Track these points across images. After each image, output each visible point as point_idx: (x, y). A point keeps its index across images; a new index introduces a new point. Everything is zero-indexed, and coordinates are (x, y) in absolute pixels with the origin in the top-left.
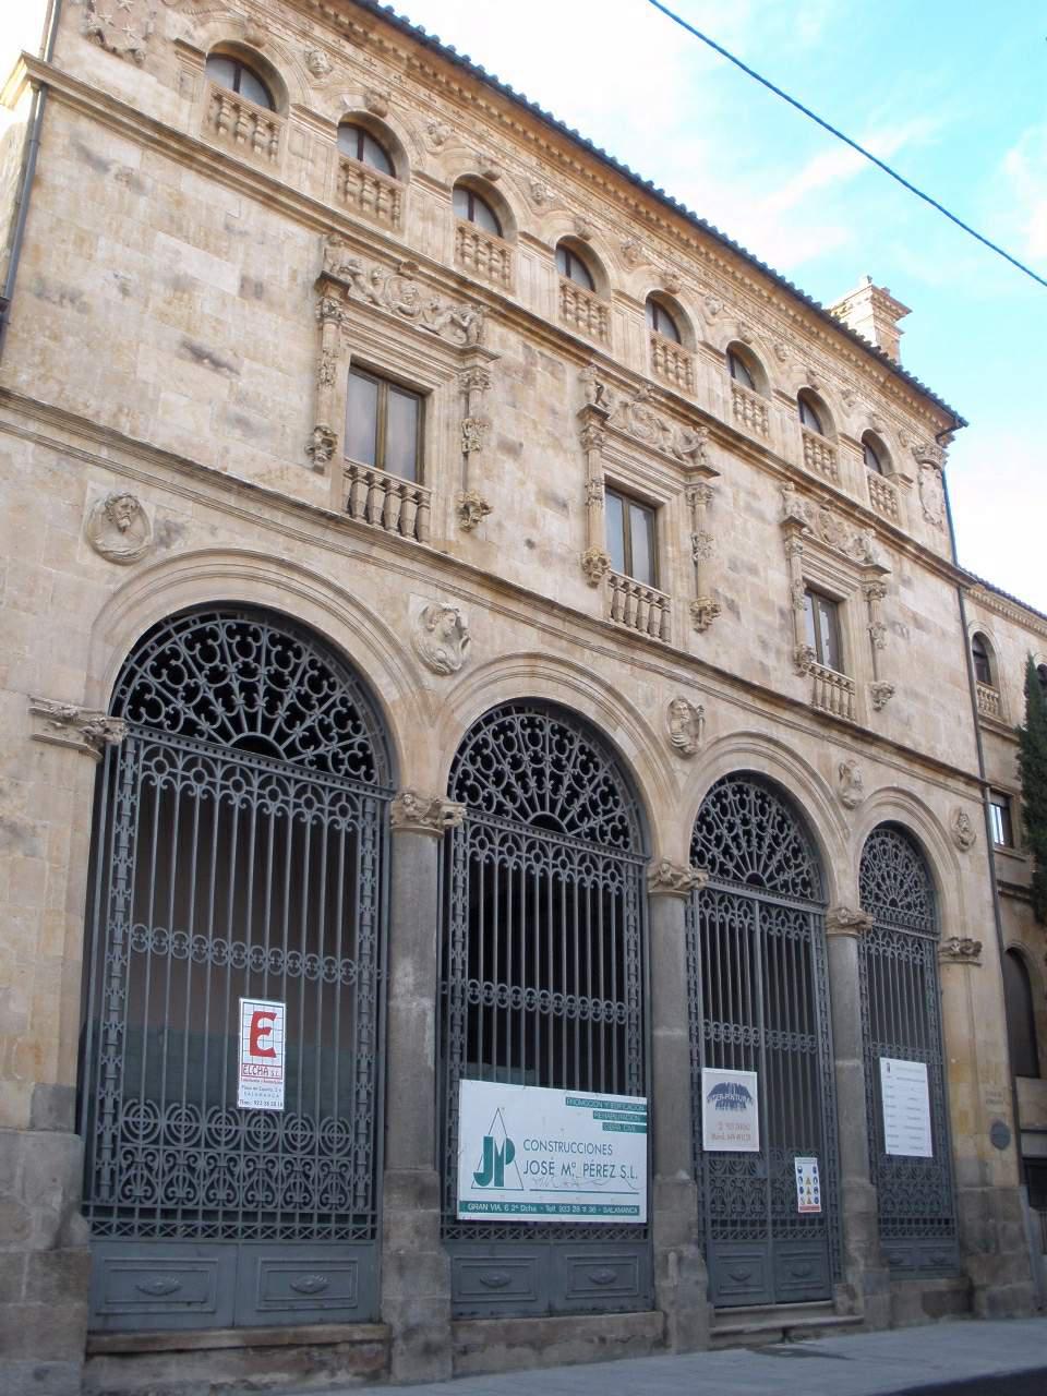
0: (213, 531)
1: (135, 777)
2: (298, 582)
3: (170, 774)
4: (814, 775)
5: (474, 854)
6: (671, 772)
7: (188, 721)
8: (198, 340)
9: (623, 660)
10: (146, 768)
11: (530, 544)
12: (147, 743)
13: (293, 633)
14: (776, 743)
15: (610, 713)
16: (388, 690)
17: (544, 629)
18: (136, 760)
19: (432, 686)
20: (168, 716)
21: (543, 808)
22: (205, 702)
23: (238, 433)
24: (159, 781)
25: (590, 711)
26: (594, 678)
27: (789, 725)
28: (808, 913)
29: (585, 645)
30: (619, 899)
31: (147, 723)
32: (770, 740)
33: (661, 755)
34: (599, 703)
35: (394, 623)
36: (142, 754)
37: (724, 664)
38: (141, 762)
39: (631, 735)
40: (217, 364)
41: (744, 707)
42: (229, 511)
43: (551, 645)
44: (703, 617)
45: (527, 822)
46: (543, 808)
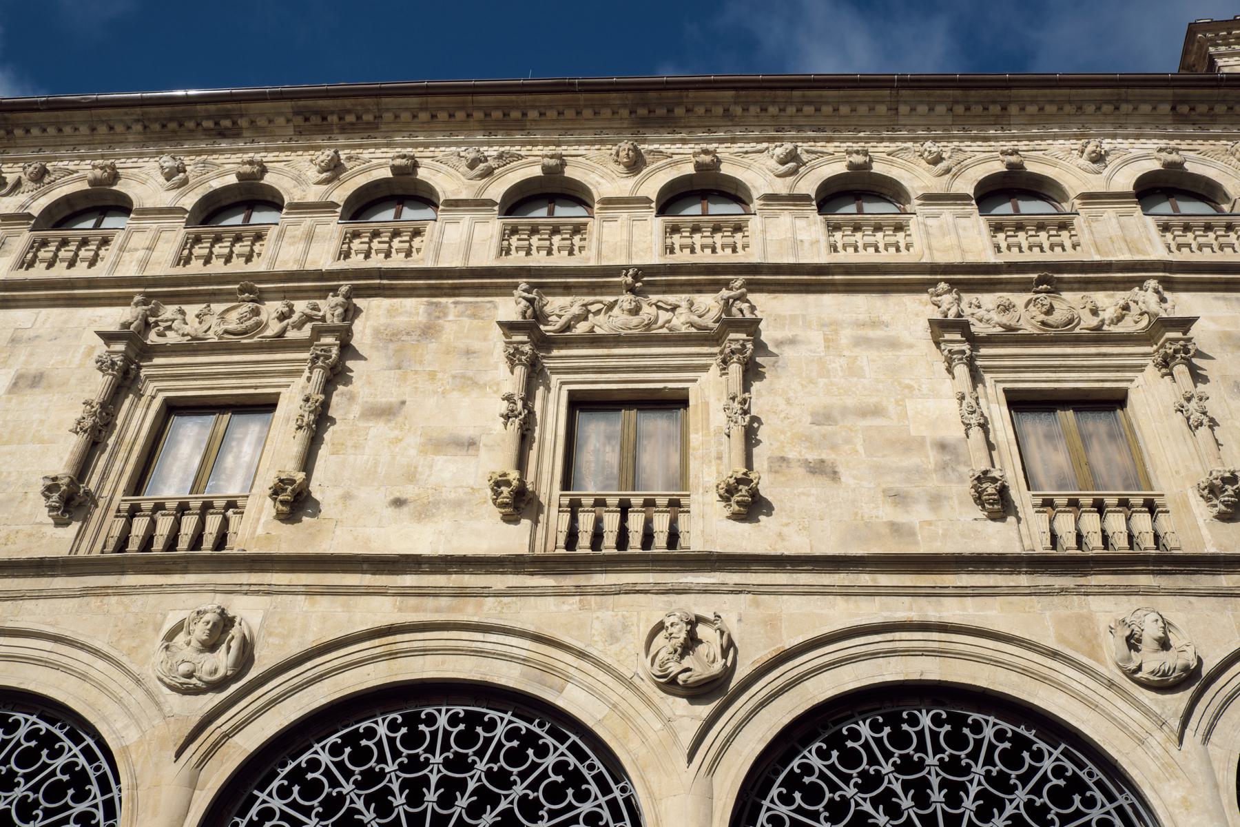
4: (1054, 655)
9: (560, 593)
11: (398, 503)
15: (547, 669)
16: (116, 729)
17: (403, 593)
19: (176, 710)
27: (961, 593)
33: (649, 702)
35: (131, 651)
39: (591, 690)
41: (824, 592)
43: (416, 609)
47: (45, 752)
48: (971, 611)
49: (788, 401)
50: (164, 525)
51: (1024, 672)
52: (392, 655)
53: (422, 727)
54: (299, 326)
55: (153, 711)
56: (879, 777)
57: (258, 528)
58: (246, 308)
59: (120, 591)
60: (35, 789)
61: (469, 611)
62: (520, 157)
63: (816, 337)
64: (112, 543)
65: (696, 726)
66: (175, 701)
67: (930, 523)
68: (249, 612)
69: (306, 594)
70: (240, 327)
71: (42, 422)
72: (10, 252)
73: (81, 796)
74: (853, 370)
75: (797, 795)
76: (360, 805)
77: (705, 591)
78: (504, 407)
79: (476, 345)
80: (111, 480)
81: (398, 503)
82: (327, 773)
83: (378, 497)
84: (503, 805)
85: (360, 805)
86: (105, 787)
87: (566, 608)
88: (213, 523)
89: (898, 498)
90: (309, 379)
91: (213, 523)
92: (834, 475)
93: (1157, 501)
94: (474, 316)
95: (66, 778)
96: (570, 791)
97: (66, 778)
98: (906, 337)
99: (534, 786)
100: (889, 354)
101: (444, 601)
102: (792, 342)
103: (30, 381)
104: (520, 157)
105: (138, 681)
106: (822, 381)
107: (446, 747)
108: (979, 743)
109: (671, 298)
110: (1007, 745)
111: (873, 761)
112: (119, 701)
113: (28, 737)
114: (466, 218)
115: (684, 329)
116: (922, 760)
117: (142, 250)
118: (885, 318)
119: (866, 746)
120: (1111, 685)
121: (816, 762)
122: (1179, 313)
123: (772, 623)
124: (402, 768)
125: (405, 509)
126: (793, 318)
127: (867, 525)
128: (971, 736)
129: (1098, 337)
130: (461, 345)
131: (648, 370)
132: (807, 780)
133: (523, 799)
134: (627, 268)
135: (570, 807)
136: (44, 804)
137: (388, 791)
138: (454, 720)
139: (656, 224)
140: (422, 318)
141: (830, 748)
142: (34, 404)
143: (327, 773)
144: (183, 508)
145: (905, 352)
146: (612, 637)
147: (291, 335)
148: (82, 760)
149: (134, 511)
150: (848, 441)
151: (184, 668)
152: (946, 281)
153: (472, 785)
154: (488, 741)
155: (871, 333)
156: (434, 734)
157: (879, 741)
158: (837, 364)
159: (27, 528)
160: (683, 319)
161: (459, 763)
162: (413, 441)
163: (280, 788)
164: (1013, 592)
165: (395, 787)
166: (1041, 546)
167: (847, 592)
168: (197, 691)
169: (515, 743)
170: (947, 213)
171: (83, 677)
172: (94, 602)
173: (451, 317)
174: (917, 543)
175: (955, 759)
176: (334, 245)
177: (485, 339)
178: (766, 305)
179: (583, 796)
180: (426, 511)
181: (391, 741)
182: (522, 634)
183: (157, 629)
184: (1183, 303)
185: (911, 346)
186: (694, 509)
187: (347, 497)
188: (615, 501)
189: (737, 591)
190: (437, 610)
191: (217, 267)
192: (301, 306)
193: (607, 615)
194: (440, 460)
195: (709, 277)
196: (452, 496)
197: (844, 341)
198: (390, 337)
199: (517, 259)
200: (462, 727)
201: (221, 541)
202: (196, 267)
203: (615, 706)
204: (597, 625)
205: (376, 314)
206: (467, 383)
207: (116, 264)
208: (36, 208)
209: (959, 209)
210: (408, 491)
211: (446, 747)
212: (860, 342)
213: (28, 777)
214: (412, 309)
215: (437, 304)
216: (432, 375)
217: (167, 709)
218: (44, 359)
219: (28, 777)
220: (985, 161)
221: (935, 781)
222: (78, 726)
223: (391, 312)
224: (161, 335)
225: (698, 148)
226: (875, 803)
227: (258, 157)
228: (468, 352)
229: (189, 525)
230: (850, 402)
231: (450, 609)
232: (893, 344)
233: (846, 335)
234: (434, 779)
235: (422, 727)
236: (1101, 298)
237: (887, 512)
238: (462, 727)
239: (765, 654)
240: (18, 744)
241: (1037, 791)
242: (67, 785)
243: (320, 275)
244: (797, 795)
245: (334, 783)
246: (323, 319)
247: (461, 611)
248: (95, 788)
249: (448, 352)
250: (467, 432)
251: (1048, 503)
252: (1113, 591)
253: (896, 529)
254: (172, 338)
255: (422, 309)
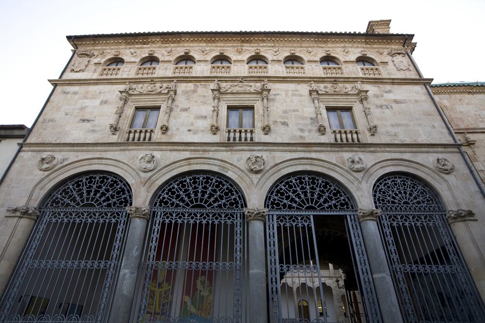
0: (77, 156)
1: (388, 224)
2: (104, 161)
3: (196, 219)
4: (335, 165)
5: (391, 224)
6: (251, 179)
7: (289, 205)
8: (84, 118)
9: (227, 151)
10: (390, 221)
11: (189, 130)
12: (388, 215)
13: (105, 175)
14: (311, 159)
15: (224, 167)
16: (130, 180)
17: (191, 151)
18: (386, 220)
20: (282, 205)
21: (309, 204)
22: (293, 199)
23: (91, 133)
24: (395, 224)
25: (215, 169)
26: (215, 159)
27: (315, 151)
28: (309, 215)
29: (209, 151)
30: (435, 227)
31: (276, 209)
32: (307, 159)
33: (247, 175)
34: (219, 166)
35: (132, 163)
36: (387, 218)
37: (279, 140)
38: (388, 220)
39: (234, 172)
40: (88, 121)
42: (78, 151)
43: (195, 154)
44: (267, 130)
45: (304, 209)
46: (309, 204)
47: (115, 185)
48: (317, 155)
49: (277, 108)
50: (137, 135)
51: (328, 168)
52: (190, 164)
53: (197, 180)
54: (164, 90)
55: (137, 176)
56: (297, 191)
57: (157, 136)
58: (152, 85)
59: (128, 150)
60: (114, 192)
61: (206, 155)
62: (214, 50)
63: (283, 93)
64: (126, 139)
65: (257, 180)
66: (142, 174)
67: (308, 136)
68: (157, 155)
69: (170, 151)
70: (151, 90)
71: (108, 112)
72: (97, 72)
73: (124, 194)
74: (292, 101)
75: (279, 194)
76: (184, 196)
77: (259, 150)
78: (213, 109)
79: (206, 94)
80: (124, 125)
81: (189, 130)
82: (176, 189)
83: (185, 129)
84: (215, 196)
85: (184, 196)
86: (129, 192)
87: (228, 154)
88: (148, 135)
89: (302, 130)
90: (168, 102)
91: (148, 135)
92: (287, 125)
93: (358, 131)
94: (205, 88)
95: (120, 190)
96: (230, 194)
97: (120, 190)
98: (304, 94)
99: (222, 193)
100: (300, 98)
101: (201, 153)
102: (278, 94)
103: (104, 102)
104: (214, 50)
105: (134, 170)
106: (285, 104)
107: (202, 184)
108: (318, 184)
109: (250, 84)
110: (324, 184)
111: (295, 187)
112: (130, 174)
113: (111, 181)
114: (202, 64)
115: (253, 91)
116: (306, 187)
117: (127, 71)
118: (299, 89)
119: (294, 184)
120: (347, 171)
121: (283, 187)
122: (365, 89)
123: (274, 158)
124: (193, 188)
125: (191, 132)
126: (278, 89)
127: (295, 136)
128: (316, 182)
129: (347, 94)
130: (202, 94)
131: (245, 100)
132: (281, 191)
133: (220, 195)
134: (240, 77)
135: (230, 197)
136: (116, 195)
137: (190, 193)
138: (204, 178)
139: (247, 66)
140: (193, 88)
141: (286, 185)
142: (106, 107)
143: (176, 189)
144: (141, 132)
145: (303, 97)
146: (238, 161)
147: (163, 92)
148: (123, 186)
149: (130, 132)
150: (290, 117)
151: (144, 167)
152: (313, 81)
153: (208, 192)
154: (211, 183)
155: (295, 93)
156: (199, 181)
157: (297, 183)
158: (288, 100)
159: (107, 136)
160: (253, 89)
161: (205, 188)
162: (192, 116)
163: (166, 192)
164: (327, 151)
165: (192, 192)
166: (333, 141)
167: (290, 151)
168: (147, 172)
169: (217, 183)
170: (313, 65)
171: (122, 169)
172: (123, 152)
173: (200, 88)
174: (306, 140)
175: (313, 187)
176: (172, 71)
177: (208, 93)
178: (270, 86)
179: (233, 195)
180: (196, 132)
181: (190, 183)
182: (218, 160)
183: (137, 158)
184: (366, 87)
185: (305, 96)
186: (256, 132)
187: (178, 129)
188: (238, 130)
189: (266, 150)
190: (199, 154)
191: (145, 76)
192: (165, 85)
193: (237, 156)
194: (199, 121)
195: (259, 79)
196: (202, 129)
197: (290, 95)
198: (186, 92)
199: (213, 75)
200: (205, 180)
201: (150, 139)
202: (140, 76)
203: (239, 176)
204: (235, 158)
205: (182, 87)
206: (204, 103)
207: (122, 75)
208: (103, 61)
209: (316, 64)
210: (191, 128)
211: (202, 184)
212: (295, 95)
213: (112, 190)
214: (191, 86)
215: (196, 85)
216: (196, 102)
217: (141, 176)
218: (107, 97)
219: (112, 190)
220: (322, 53)
221: (309, 192)
222: (122, 180)
223: (186, 87)
224: (133, 92)
225: (256, 49)
226: (296, 196)
227: (153, 49)
228: (204, 96)
229: (142, 135)
230: (291, 108)
231: (202, 154)
232: (301, 95)
233: (290, 93)
234: (200, 191)
235: (197, 180)
236: (347, 85)
237: (299, 133)
238: (205, 180)
239: (273, 164)
240: (109, 183)
241: (330, 193)
242: (121, 191)
243: (170, 78)
244: (279, 194)
245: (178, 192)
246: (170, 88)
247: (204, 154)
248: (126, 192)
249: (199, 96)
250: (204, 115)
251: (334, 132)
252: (348, 151)
253: (301, 137)
254: (135, 93)
255: (193, 86)
